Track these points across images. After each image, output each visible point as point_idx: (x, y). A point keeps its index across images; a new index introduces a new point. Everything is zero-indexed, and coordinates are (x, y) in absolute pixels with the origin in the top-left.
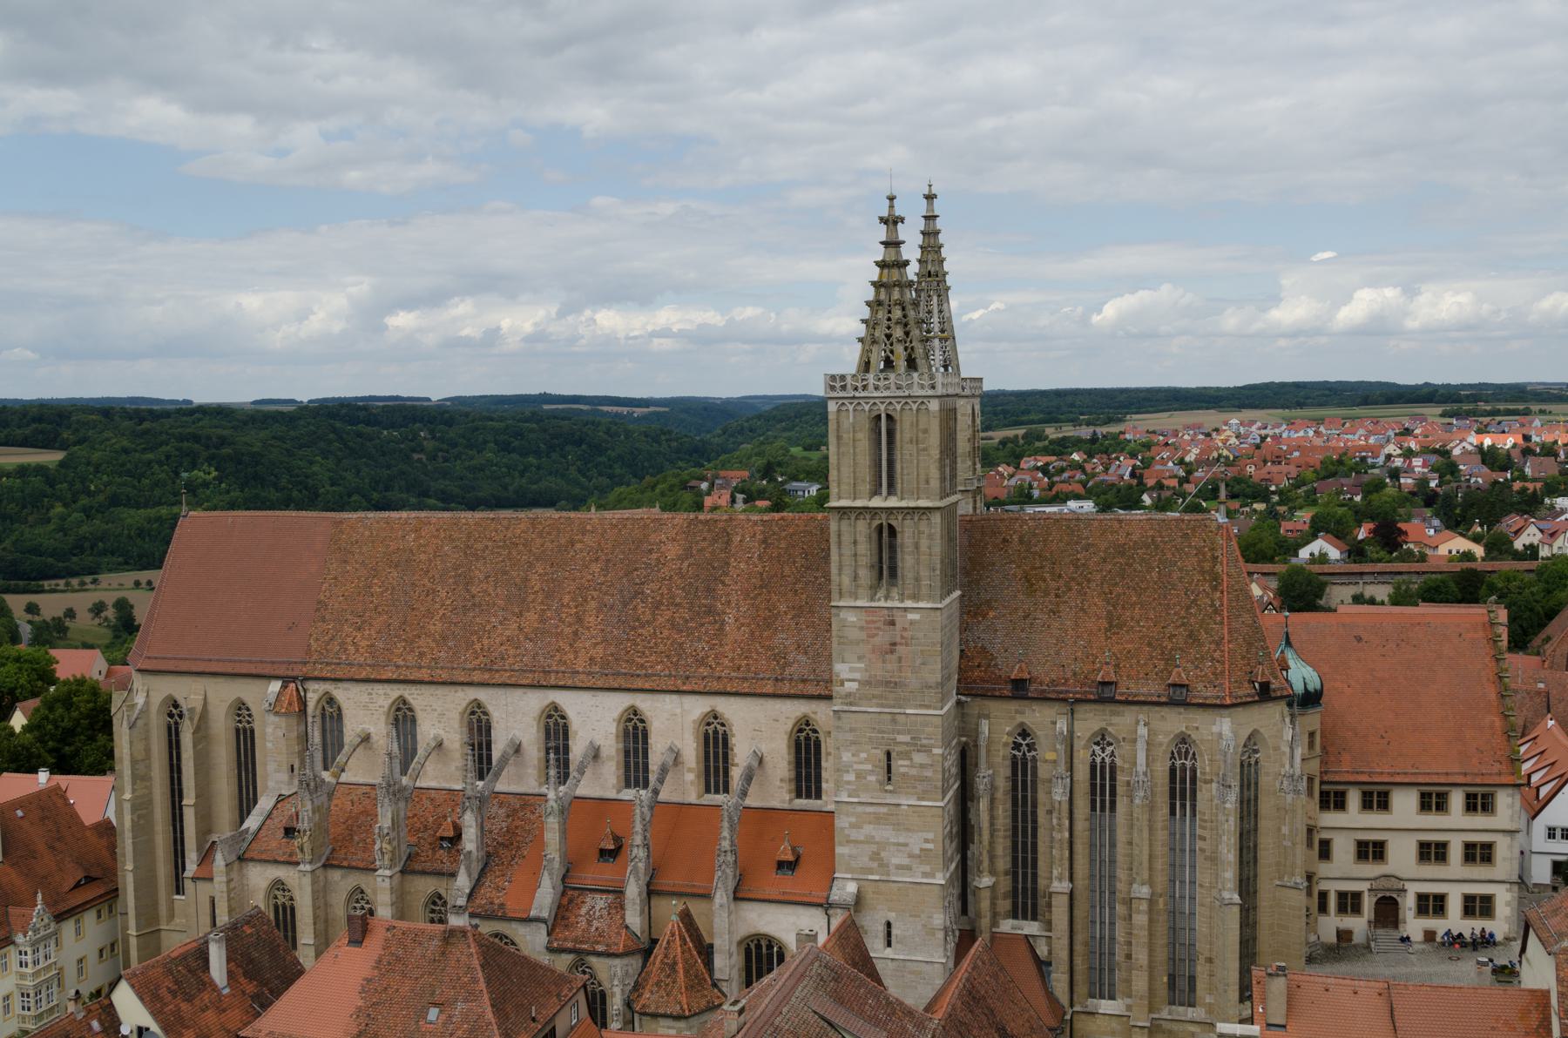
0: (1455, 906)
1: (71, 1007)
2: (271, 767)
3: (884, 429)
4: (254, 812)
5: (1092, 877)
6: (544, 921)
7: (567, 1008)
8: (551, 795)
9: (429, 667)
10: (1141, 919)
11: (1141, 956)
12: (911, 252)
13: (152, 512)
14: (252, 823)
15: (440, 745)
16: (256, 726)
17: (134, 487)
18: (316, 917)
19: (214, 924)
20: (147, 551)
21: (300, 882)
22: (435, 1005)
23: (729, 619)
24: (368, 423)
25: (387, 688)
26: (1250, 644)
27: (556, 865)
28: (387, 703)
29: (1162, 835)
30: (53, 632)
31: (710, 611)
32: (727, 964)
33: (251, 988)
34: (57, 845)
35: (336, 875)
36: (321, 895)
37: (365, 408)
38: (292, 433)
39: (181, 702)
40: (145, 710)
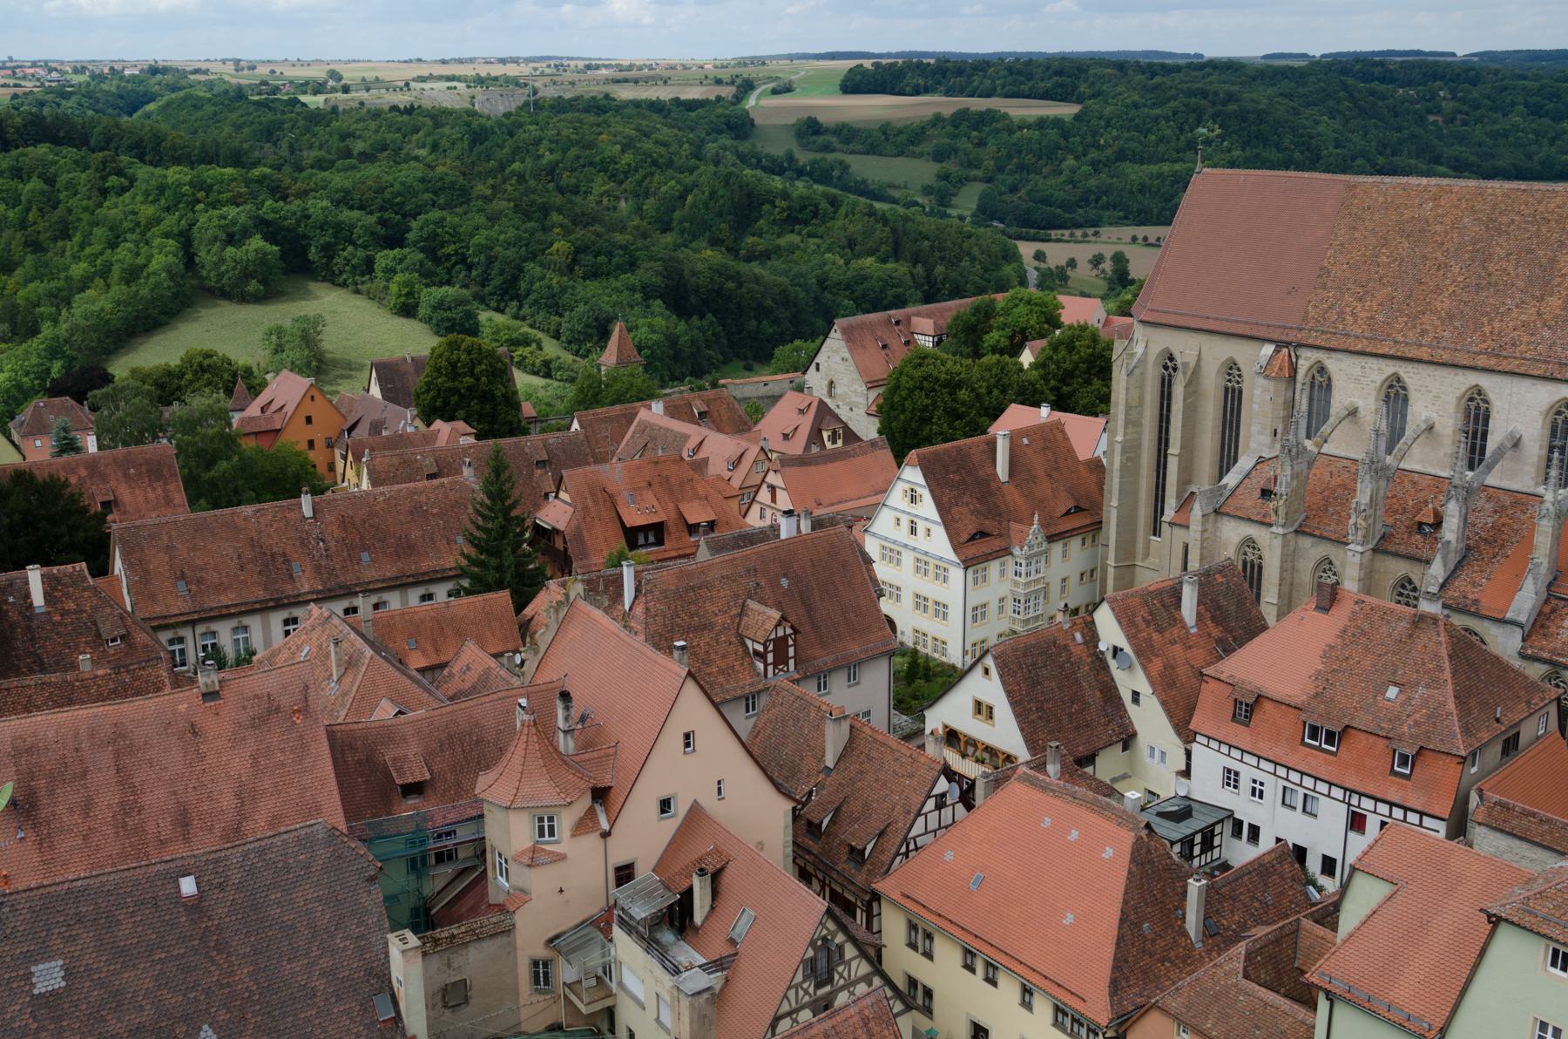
2: (1255, 428)
4: (1234, 470)
6: (1520, 625)
7: (1536, 717)
8: (1549, 497)
9: (1429, 346)
13: (1154, 168)
14: (1231, 479)
15: (1431, 428)
16: (1245, 387)
17: (1140, 142)
18: (1282, 579)
19: (1185, 568)
20: (1156, 206)
21: (1271, 545)
22: (1396, 684)
24: (1383, 80)
25: (1382, 363)
27: (1543, 570)
28: (1379, 379)
30: (1056, 279)
33: (1216, 632)
34: (1054, 474)
35: (1306, 542)
36: (1289, 559)
37: (1382, 64)
38: (1301, 90)
39: (1177, 355)
40: (1143, 360)
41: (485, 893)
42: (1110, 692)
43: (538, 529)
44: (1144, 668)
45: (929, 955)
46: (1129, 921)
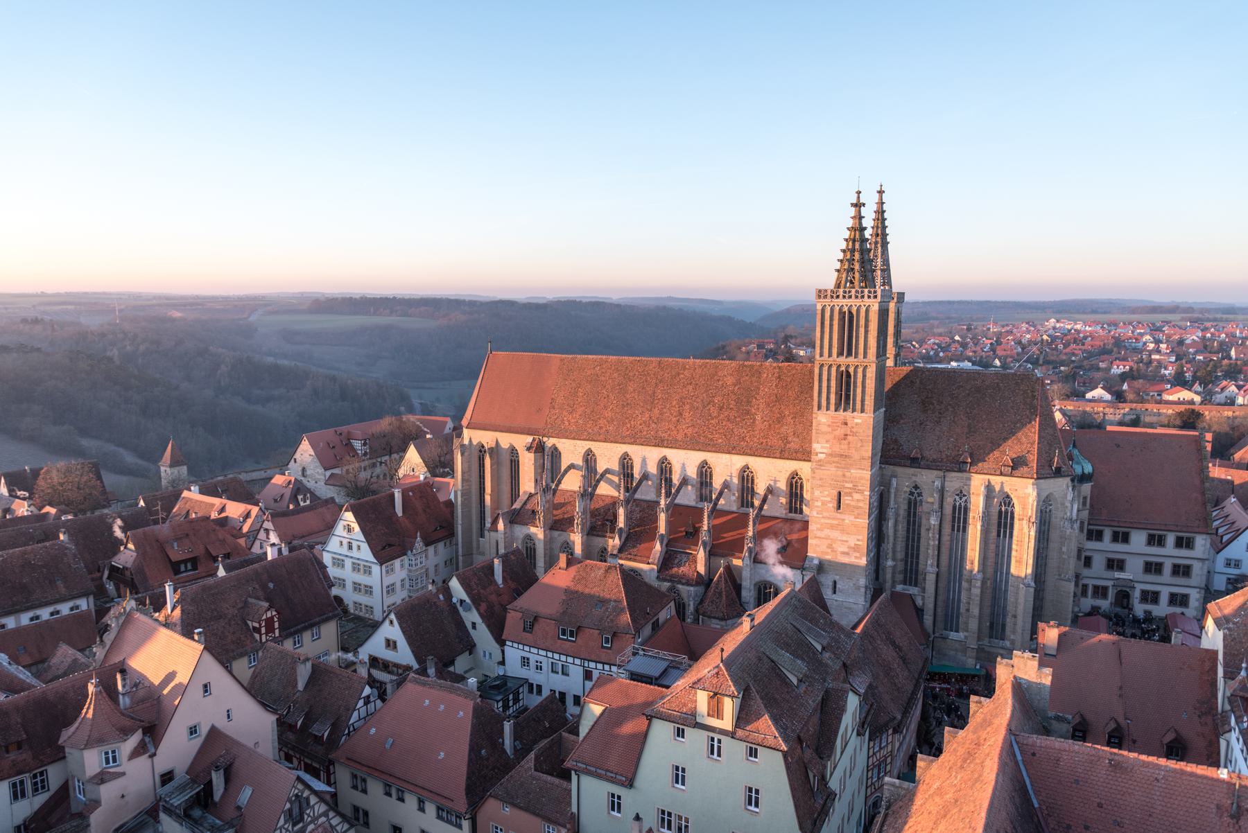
0: (1164, 598)
1: (430, 587)
3: (848, 321)
5: (950, 566)
10: (976, 591)
11: (975, 611)
12: (868, 222)
14: (517, 505)
23: (758, 418)
26: (1050, 445)
29: (992, 547)
31: (748, 412)
32: (748, 594)
33: (513, 585)
41: (69, 807)
42: (460, 623)
43: (114, 569)
44: (478, 610)
45: (365, 791)
46: (474, 749)
